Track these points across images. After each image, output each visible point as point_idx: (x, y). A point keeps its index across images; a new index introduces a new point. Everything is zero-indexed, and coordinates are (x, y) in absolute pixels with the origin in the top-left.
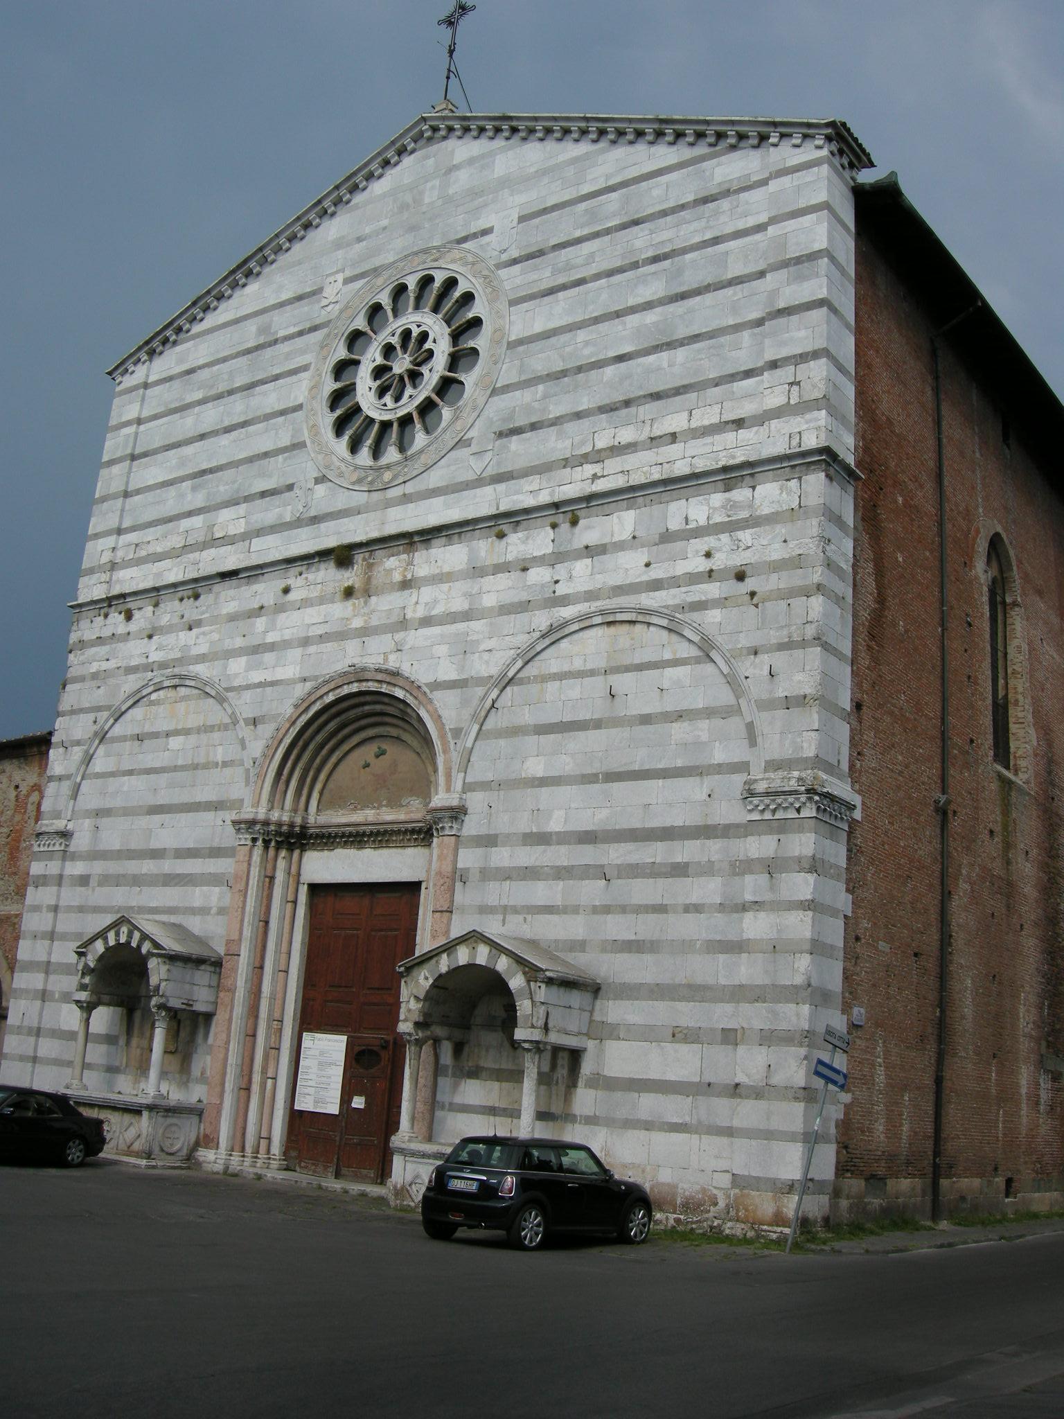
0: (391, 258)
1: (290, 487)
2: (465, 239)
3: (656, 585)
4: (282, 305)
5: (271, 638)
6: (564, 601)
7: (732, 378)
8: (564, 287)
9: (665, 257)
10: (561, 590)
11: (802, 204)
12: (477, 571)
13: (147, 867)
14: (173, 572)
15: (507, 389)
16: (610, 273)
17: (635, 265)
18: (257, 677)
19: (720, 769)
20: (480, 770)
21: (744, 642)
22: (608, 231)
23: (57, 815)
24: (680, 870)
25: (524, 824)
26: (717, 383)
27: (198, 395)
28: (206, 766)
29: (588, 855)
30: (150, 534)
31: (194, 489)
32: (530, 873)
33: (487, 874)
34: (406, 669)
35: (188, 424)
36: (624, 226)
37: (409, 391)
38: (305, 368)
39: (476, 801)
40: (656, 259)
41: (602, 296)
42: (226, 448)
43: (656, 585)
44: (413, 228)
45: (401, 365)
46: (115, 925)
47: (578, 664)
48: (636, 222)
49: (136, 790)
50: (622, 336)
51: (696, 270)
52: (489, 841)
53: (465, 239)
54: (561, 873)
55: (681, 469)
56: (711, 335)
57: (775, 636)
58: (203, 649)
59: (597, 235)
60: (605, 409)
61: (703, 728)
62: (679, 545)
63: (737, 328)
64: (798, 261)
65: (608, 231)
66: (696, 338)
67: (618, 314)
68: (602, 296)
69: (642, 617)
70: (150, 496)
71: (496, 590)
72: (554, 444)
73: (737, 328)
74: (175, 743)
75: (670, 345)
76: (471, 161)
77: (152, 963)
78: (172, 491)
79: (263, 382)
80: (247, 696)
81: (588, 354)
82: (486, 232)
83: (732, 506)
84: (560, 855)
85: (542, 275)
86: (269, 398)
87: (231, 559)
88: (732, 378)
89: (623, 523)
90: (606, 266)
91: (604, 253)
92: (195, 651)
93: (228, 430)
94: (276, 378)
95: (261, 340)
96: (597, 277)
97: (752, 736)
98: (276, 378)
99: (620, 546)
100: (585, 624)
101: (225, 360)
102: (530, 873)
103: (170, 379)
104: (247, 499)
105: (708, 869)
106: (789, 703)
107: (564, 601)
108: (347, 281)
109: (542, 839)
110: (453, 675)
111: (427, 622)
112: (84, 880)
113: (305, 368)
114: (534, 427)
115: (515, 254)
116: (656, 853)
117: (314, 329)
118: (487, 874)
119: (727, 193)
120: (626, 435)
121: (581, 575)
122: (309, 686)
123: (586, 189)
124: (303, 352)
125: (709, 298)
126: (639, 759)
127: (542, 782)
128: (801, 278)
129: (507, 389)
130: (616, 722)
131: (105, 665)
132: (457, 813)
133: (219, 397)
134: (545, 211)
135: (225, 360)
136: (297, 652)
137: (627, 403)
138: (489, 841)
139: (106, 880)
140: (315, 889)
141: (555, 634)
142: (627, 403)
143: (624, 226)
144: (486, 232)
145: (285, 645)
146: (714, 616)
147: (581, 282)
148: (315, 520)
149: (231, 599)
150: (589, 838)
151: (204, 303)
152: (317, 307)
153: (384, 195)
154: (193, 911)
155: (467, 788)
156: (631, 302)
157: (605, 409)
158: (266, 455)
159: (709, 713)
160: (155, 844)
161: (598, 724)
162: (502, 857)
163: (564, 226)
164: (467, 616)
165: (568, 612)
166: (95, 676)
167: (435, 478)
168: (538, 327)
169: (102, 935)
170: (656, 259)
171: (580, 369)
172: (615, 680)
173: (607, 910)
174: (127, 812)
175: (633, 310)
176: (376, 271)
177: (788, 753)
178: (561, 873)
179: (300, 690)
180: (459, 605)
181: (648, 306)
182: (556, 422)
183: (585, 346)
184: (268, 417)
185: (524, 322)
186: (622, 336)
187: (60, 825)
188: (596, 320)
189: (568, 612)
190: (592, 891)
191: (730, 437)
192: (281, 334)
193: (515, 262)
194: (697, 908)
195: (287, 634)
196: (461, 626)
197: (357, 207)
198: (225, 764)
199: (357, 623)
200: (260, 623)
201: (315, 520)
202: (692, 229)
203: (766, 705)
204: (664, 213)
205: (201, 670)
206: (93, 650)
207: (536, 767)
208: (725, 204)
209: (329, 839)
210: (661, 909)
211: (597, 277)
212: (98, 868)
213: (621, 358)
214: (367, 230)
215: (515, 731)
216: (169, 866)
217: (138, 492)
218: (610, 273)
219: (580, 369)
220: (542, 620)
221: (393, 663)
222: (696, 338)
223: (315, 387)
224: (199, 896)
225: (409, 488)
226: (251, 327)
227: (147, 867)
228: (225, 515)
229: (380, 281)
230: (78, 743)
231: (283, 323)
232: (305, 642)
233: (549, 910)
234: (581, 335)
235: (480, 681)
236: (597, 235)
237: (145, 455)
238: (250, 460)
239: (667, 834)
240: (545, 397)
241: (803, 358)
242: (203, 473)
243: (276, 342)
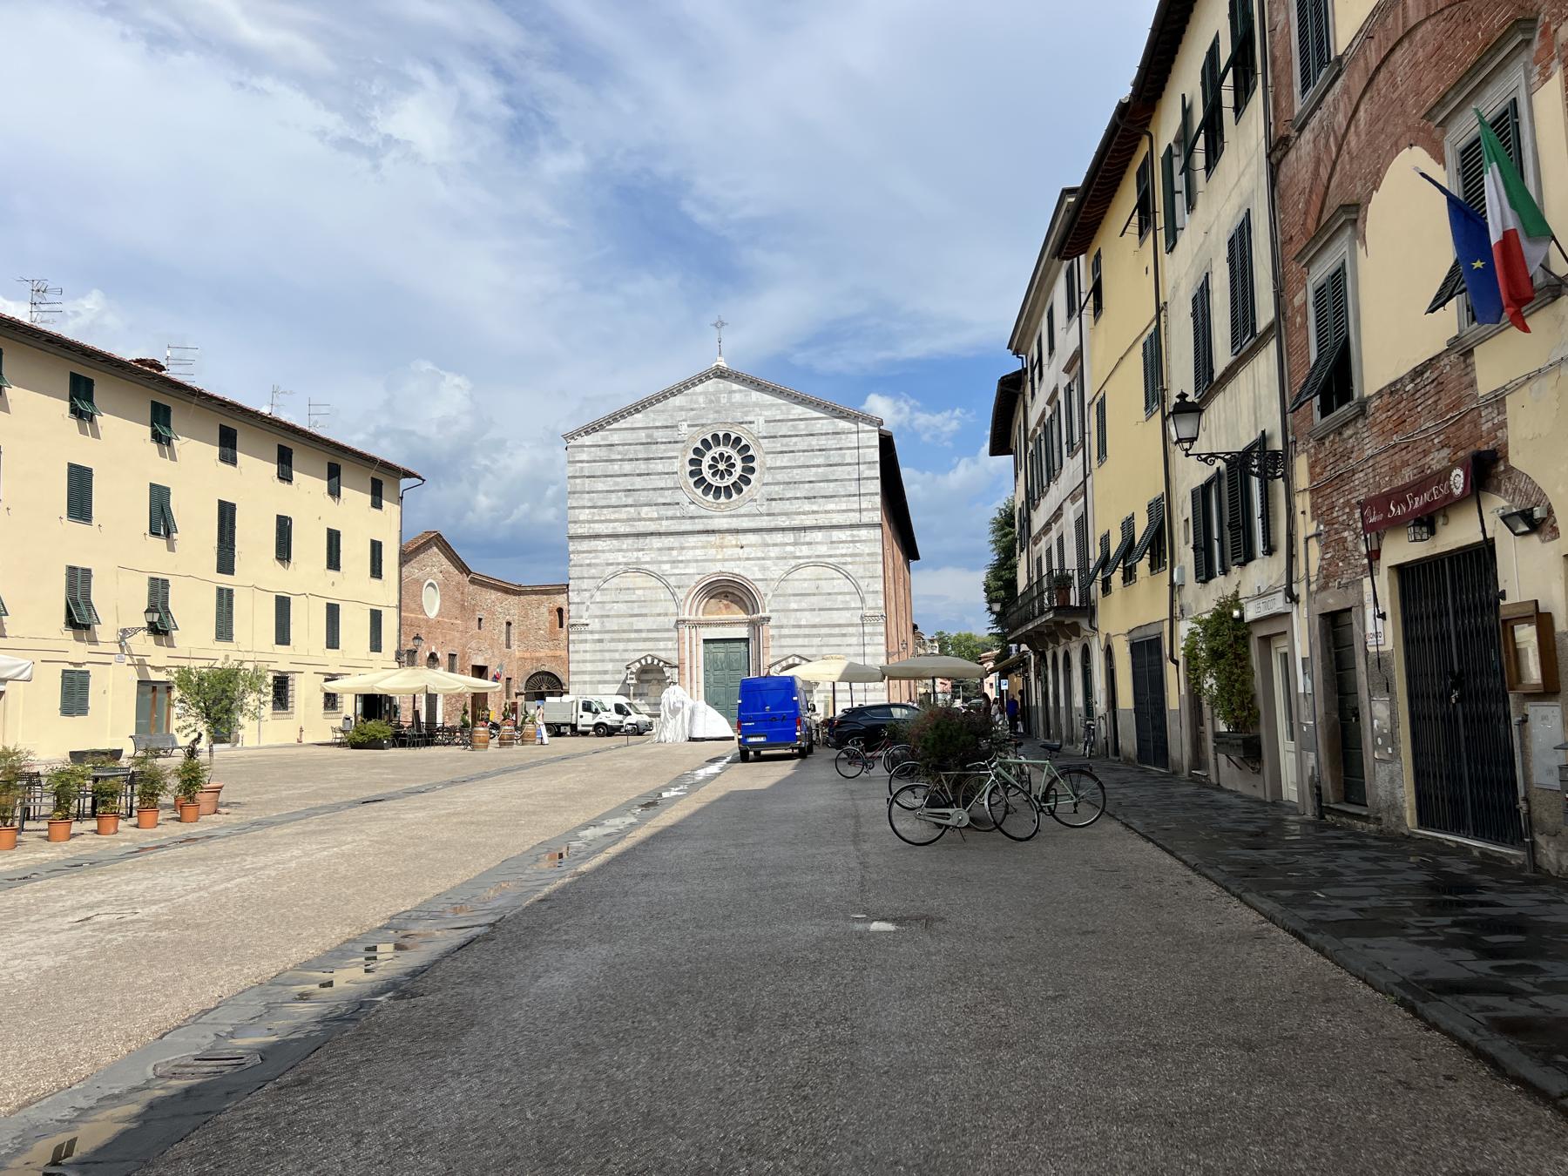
0: (709, 422)
1: (678, 504)
2: (742, 423)
3: (830, 556)
4: (657, 428)
5: (680, 558)
6: (799, 558)
7: (850, 496)
8: (786, 452)
9: (823, 450)
10: (798, 554)
11: (870, 444)
12: (767, 545)
13: (633, 635)
14: (622, 529)
15: (767, 484)
16: (804, 451)
17: (813, 451)
18: (677, 571)
19: (854, 609)
20: (774, 606)
21: (859, 575)
22: (801, 436)
23: (581, 617)
24: (844, 635)
25: (792, 622)
26: (844, 496)
27: (620, 457)
28: (656, 601)
29: (814, 631)
30: (605, 511)
31: (626, 496)
32: (797, 636)
33: (781, 636)
34: (742, 574)
35: (616, 468)
36: (807, 435)
37: (726, 477)
38: (676, 457)
39: (773, 615)
40: (820, 450)
41: (802, 459)
42: (639, 482)
43: (830, 556)
44: (717, 412)
45: (722, 466)
46: (645, 658)
47: (805, 577)
48: (812, 435)
49: (622, 608)
50: (811, 474)
51: (835, 457)
52: (782, 627)
53: (742, 423)
54: (806, 636)
55: (835, 522)
56: (841, 480)
57: (868, 574)
58: (648, 559)
59: (797, 436)
60: (805, 498)
61: (848, 597)
62: (836, 545)
63: (850, 480)
64: (869, 463)
65: (801, 436)
66: (836, 480)
67: (808, 466)
68: (802, 459)
69: (827, 565)
70: (601, 495)
71: (774, 552)
72: (786, 506)
73: (850, 480)
74: (637, 592)
75: (828, 481)
76: (740, 391)
77: (665, 669)
78: (613, 495)
79: (653, 459)
80: (673, 578)
81: (798, 478)
82: (750, 423)
83: (853, 536)
84: (807, 631)
85: (778, 445)
86: (659, 466)
87: (652, 527)
88: (850, 496)
89: (818, 536)
90: (801, 448)
91: (802, 443)
92: (643, 560)
93: (639, 475)
94: (661, 458)
95: (649, 441)
96: (799, 451)
97: (862, 600)
98: (661, 458)
99: (817, 543)
100: (807, 565)
101: (630, 444)
102: (797, 636)
103: (600, 446)
104: (655, 505)
105: (852, 635)
106: (873, 592)
107: (799, 558)
108: (689, 426)
109: (800, 626)
110: (762, 577)
111: (748, 559)
112: (601, 641)
113: (676, 457)
114: (780, 499)
115: (765, 435)
116: (836, 631)
117: (676, 442)
118: (781, 636)
119: (844, 433)
120: (815, 508)
121: (805, 550)
122: (701, 576)
123: (791, 417)
124: (673, 451)
125: (840, 468)
126: (828, 604)
127: (797, 610)
128: (869, 469)
129: (767, 484)
130: (820, 594)
131: (593, 561)
132: (769, 619)
133: (631, 460)
134: (775, 421)
135: (630, 444)
136: (695, 564)
137: (815, 497)
138: (782, 627)
139: (612, 640)
140: (706, 641)
141: (797, 567)
142: (815, 497)
143: (807, 435)
144: (750, 423)
145: (689, 561)
146: (850, 567)
147: (793, 452)
148: (691, 518)
149: (656, 542)
150: (814, 626)
151: (614, 418)
152: (676, 433)
153: (701, 394)
154: (660, 650)
155: (771, 611)
156: (812, 463)
157: (805, 498)
158: (662, 489)
159: (849, 593)
160: (635, 628)
161: (814, 595)
162: (785, 631)
163: (784, 429)
164: (763, 559)
165: (801, 561)
166: (589, 565)
167: (742, 511)
168: (778, 464)
169: (639, 661)
170: (820, 450)
171: (795, 483)
172: (819, 582)
173: (822, 646)
174: (618, 616)
175: (813, 466)
176: (703, 425)
177: (873, 605)
178: (806, 636)
179: (698, 578)
180: (760, 554)
181: (819, 466)
182: (788, 499)
183: (797, 474)
184: (659, 474)
185: (770, 461)
186: (811, 474)
187: (583, 621)
188: (800, 467)
189: (801, 561)
190: (816, 641)
191: (851, 515)
192: (659, 440)
193: (765, 437)
194: (850, 645)
195: (688, 558)
196: (763, 562)
197: (687, 394)
198: (665, 600)
199: (719, 557)
200: (675, 553)
201: (691, 518)
202: (831, 442)
203: (868, 592)
204: (822, 434)
205: (647, 566)
206: (585, 555)
207: (794, 606)
208: (843, 436)
209: (708, 624)
210: (839, 645)
211: (799, 451)
212: (607, 636)
213: (810, 482)
214: (695, 406)
215: (784, 595)
216: (644, 635)
217: (593, 492)
218: (804, 451)
219: (795, 483)
220: (793, 562)
221: (736, 571)
222: (836, 480)
223: (683, 466)
224: (662, 645)
225: (733, 512)
226: (643, 434)
227: (633, 635)
228: (645, 509)
229: (705, 430)
230: (586, 590)
231: (659, 435)
232: (697, 561)
233: (804, 646)
234: (795, 471)
235: (773, 580)
236: (797, 436)
237: (593, 477)
238: (654, 489)
239: (839, 626)
240: (783, 489)
241: (872, 494)
242: (629, 490)
243: (657, 443)
